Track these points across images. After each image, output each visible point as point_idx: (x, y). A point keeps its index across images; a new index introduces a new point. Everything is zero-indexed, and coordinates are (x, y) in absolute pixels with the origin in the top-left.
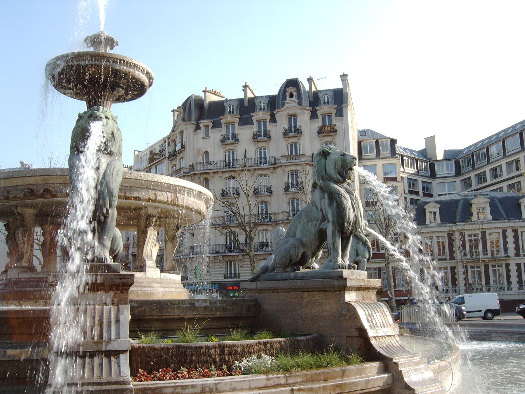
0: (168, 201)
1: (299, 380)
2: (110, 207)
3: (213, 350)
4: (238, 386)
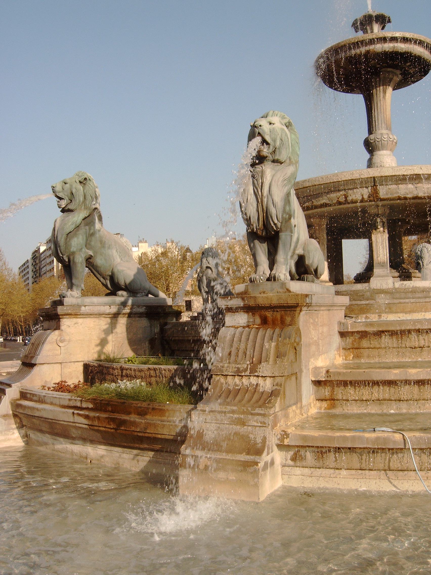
0: (363, 198)
1: (91, 406)
2: (62, 255)
3: (116, 371)
4: (55, 401)
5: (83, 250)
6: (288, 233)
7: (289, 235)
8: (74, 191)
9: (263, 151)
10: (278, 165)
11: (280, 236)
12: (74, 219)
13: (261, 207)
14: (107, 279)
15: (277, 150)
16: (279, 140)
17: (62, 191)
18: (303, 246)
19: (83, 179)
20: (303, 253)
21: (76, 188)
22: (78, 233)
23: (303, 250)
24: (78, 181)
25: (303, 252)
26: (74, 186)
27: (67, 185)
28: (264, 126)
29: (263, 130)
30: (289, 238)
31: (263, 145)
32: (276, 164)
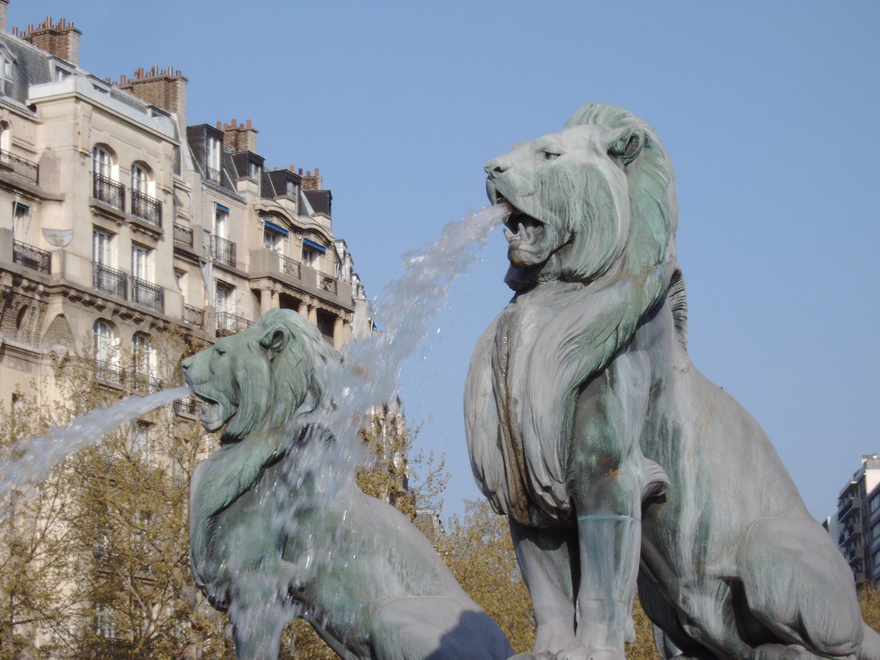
5: (269, 563)
6: (605, 514)
7: (609, 520)
8: (241, 375)
9: (517, 249)
10: (575, 289)
11: (581, 527)
12: (233, 467)
13: (508, 433)
14: (363, 655)
15: (578, 238)
16: (578, 207)
17: (210, 379)
18: (736, 547)
19: (271, 336)
20: (738, 572)
21: (245, 368)
22: (249, 510)
23: (738, 562)
24: (255, 344)
25: (734, 568)
26: (240, 361)
27: (225, 359)
28: (510, 171)
29: (507, 183)
30: (608, 531)
31: (515, 230)
32: (571, 285)
